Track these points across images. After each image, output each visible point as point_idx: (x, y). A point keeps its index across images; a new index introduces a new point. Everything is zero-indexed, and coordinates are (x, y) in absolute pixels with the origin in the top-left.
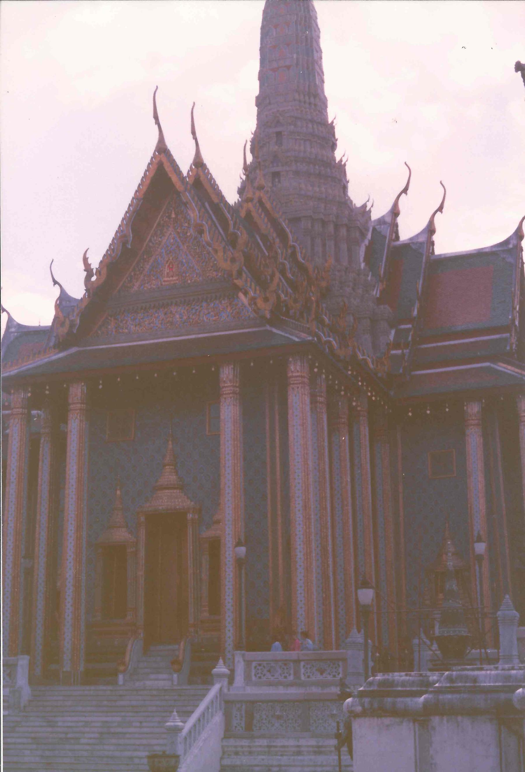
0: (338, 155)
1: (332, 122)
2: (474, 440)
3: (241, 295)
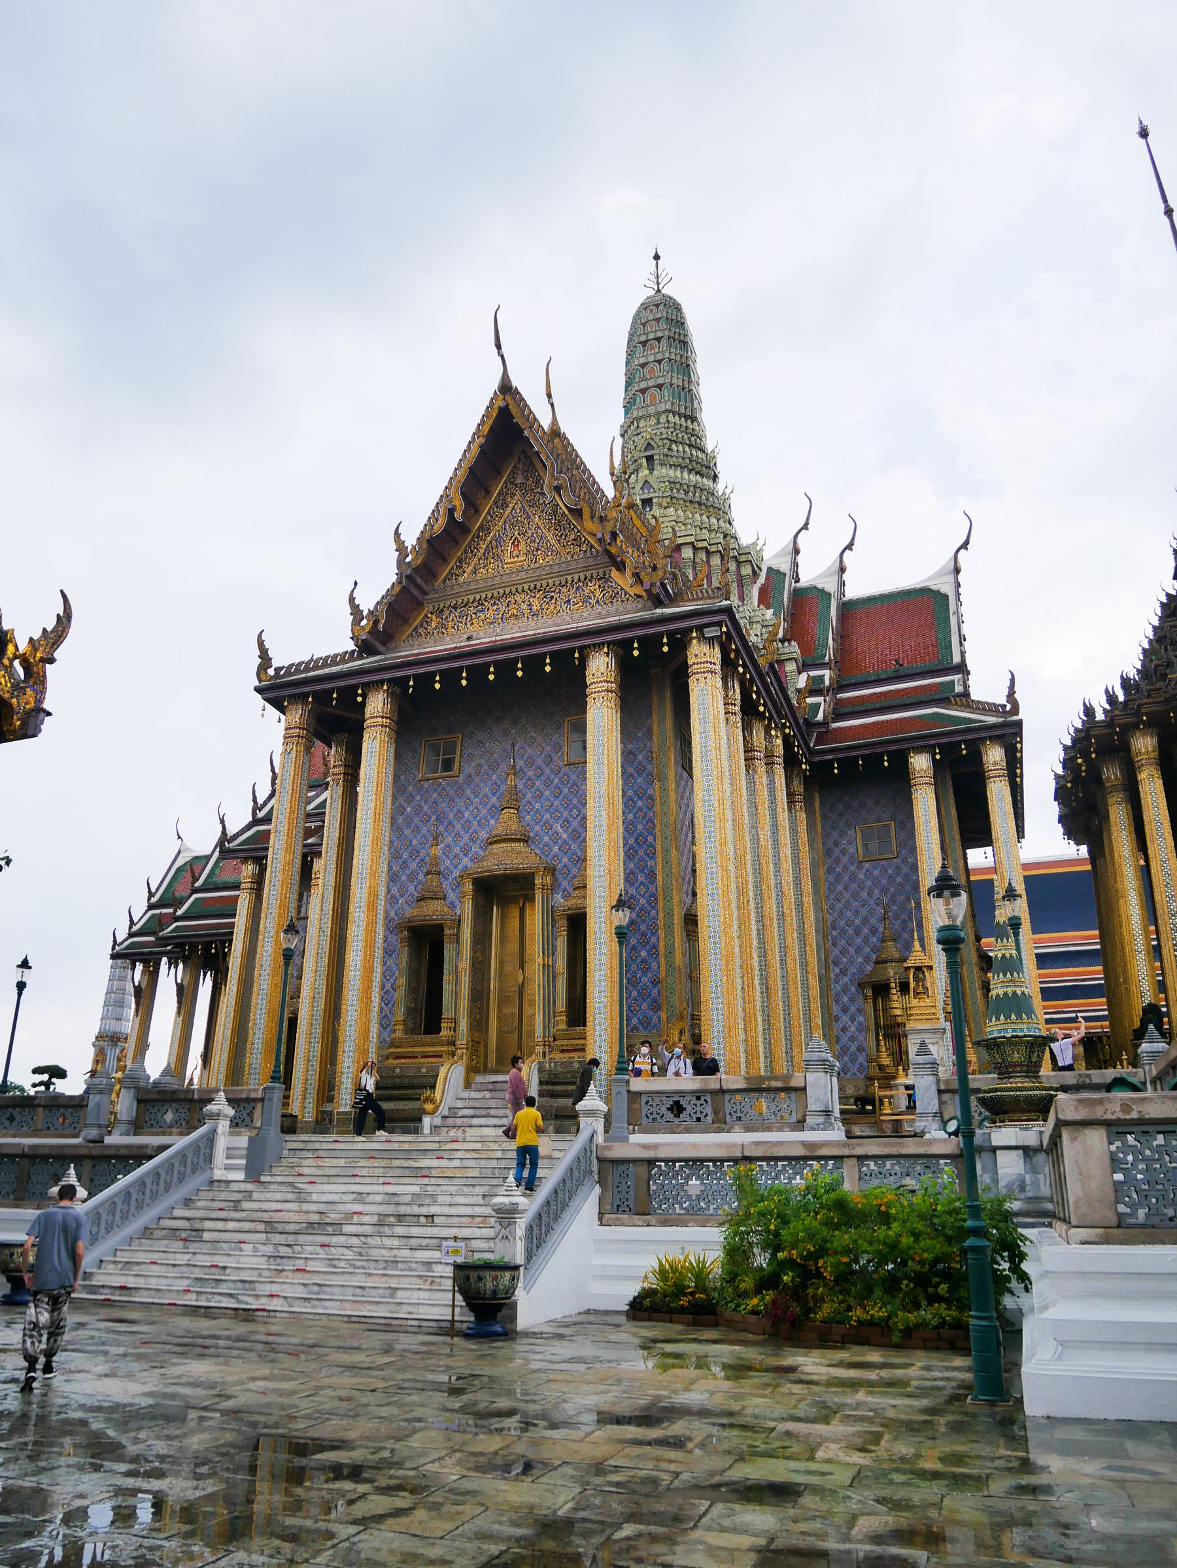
0: (720, 487)
1: (713, 451)
2: (925, 802)
3: (615, 574)
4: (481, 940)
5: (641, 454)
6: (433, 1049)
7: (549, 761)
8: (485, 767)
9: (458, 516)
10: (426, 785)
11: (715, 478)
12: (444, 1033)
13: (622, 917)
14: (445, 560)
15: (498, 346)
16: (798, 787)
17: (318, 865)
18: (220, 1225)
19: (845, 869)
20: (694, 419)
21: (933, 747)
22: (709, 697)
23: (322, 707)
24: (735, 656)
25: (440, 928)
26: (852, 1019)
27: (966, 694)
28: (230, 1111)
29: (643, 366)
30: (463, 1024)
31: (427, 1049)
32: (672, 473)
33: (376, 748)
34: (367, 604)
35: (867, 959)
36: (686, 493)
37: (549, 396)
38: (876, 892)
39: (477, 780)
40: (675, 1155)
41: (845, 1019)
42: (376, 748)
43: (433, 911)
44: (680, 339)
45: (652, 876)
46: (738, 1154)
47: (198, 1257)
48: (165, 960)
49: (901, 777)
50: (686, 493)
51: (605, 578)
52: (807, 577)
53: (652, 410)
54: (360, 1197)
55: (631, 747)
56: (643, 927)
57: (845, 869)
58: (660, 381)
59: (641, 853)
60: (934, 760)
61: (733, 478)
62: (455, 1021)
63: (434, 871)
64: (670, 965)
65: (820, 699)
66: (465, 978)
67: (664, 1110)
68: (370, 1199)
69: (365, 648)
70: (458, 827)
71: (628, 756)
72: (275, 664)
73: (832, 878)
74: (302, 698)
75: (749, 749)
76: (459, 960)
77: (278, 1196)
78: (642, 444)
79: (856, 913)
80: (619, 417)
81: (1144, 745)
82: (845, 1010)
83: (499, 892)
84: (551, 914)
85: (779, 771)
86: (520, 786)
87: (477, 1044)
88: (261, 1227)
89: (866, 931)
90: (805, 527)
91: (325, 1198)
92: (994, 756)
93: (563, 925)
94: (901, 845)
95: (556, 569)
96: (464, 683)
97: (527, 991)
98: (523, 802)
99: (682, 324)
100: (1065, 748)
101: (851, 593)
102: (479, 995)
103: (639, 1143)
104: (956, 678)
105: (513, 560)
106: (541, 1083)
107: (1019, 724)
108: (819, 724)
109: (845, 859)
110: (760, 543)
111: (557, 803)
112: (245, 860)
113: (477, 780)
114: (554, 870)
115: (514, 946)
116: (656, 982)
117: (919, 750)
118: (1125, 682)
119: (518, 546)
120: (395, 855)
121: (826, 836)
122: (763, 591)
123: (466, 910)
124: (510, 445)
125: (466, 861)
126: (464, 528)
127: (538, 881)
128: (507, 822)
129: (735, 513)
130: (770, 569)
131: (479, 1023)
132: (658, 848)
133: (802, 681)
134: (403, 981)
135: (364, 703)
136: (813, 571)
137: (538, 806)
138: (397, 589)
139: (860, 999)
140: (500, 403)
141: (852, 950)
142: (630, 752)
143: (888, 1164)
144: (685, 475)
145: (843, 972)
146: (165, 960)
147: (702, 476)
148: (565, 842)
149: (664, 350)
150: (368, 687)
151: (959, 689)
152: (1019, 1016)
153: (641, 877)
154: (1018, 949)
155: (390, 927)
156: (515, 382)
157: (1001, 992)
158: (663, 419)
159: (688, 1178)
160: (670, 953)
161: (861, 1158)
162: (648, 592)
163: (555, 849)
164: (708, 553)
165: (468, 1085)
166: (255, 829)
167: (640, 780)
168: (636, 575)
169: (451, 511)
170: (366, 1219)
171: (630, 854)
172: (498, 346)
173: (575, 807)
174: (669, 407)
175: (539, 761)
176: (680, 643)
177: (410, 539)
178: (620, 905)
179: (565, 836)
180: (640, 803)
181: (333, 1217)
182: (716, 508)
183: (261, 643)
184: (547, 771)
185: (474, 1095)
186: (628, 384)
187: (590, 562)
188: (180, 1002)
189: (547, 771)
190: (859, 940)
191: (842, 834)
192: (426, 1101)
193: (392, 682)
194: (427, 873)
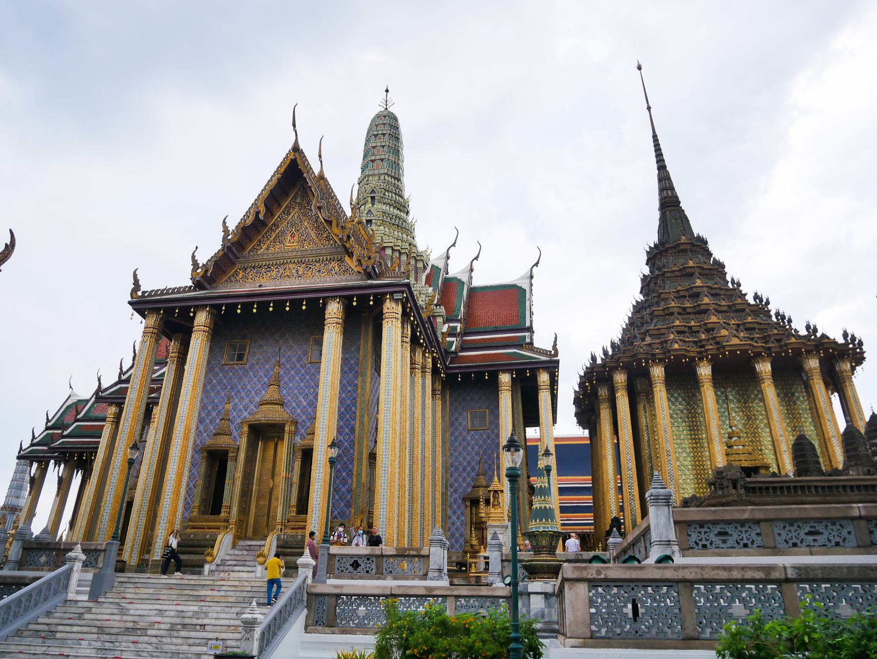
2: (506, 400)
3: (347, 258)
4: (250, 460)
5: (368, 194)
6: (215, 524)
7: (299, 359)
8: (262, 360)
9: (261, 216)
10: (226, 368)
11: (408, 213)
12: (222, 514)
13: (334, 452)
14: (251, 240)
15: (294, 125)
16: (438, 387)
17: (156, 410)
18: (68, 629)
19: (460, 434)
20: (399, 180)
21: (512, 370)
22: (393, 332)
23: (169, 317)
24: (410, 311)
25: (226, 452)
26: (458, 518)
27: (531, 343)
28: (83, 557)
29: (374, 147)
30: (235, 510)
31: (211, 524)
32: (384, 207)
33: (198, 344)
34: (202, 260)
35: (468, 485)
36: (391, 219)
37: (320, 156)
38: (476, 448)
39: (257, 367)
40: (352, 592)
41: (454, 518)
42: (198, 344)
43: (223, 441)
44: (396, 136)
45: (353, 430)
46: (388, 592)
47: (50, 649)
48: (52, 461)
49: (493, 386)
50: (391, 219)
51: (341, 260)
52: (452, 273)
53: (376, 172)
54: (161, 612)
55: (347, 356)
56: (345, 459)
57: (460, 434)
58: (383, 157)
59: (348, 416)
60: (512, 377)
61: (416, 214)
62: (230, 508)
63: (226, 419)
64: (359, 482)
65: (454, 339)
66: (238, 483)
67: (348, 565)
68: (167, 613)
69: (198, 285)
70: (243, 394)
71: (345, 361)
72: (143, 289)
73: (453, 438)
74: (157, 310)
75: (413, 363)
76: (236, 472)
77: (109, 611)
78: (369, 189)
79: (465, 458)
80: (358, 174)
81: (620, 378)
82: (454, 513)
83: (263, 433)
84: (293, 448)
85: (429, 376)
86: (282, 372)
87: (242, 523)
88: (95, 630)
89: (469, 469)
90: (454, 245)
91: (138, 613)
92: (544, 378)
93: (299, 454)
94: (491, 423)
95: (314, 252)
96: (255, 311)
97: (274, 493)
98: (282, 383)
99: (397, 128)
100: (581, 377)
101: (476, 283)
102: (246, 493)
103: (332, 584)
104: (527, 334)
105: (290, 244)
106: (278, 547)
107: (558, 362)
108: (452, 352)
109: (460, 428)
110: (429, 251)
111: (302, 384)
112: (111, 404)
113: (257, 367)
114: (297, 423)
115: (269, 465)
116: (350, 491)
117: (504, 371)
118: (613, 345)
119: (294, 237)
120: (203, 407)
121: (451, 415)
122: (428, 277)
123: (243, 443)
124: (294, 181)
125: (246, 414)
126: (263, 224)
127: (287, 428)
128: (272, 393)
129: (417, 233)
130: (433, 265)
131: (244, 510)
132: (358, 414)
133: (445, 328)
134: (201, 482)
135: (193, 318)
136: (456, 269)
137: (291, 385)
138: (221, 254)
139: (463, 507)
140: (292, 157)
141: (461, 480)
142: (347, 359)
143: (472, 600)
144: (392, 209)
145: (455, 491)
146: (52, 461)
147: (401, 211)
148: (305, 407)
149: (386, 141)
150: (197, 308)
151: (528, 340)
152: (547, 520)
153: (347, 430)
154: (549, 483)
155: (197, 449)
156: (301, 147)
157: (538, 506)
158: (382, 177)
159: (359, 605)
160: (359, 474)
161: (457, 597)
162: (365, 270)
163: (299, 411)
164: (400, 253)
165: (234, 546)
166: (119, 386)
167: (351, 375)
168: (359, 261)
169: (258, 213)
170: (163, 626)
171: (341, 416)
172: (294, 125)
173: (312, 387)
174: (386, 171)
175: (294, 360)
176: (380, 301)
177: (232, 226)
178: (333, 445)
179: (305, 404)
180: (349, 388)
181: (142, 625)
182: (406, 229)
183: (135, 276)
184: (298, 366)
185: (237, 552)
186: (365, 156)
187: (334, 250)
188: (59, 488)
189: (298, 366)
190: (465, 474)
191: (460, 414)
192: (208, 555)
193: (212, 306)
194: (222, 419)
